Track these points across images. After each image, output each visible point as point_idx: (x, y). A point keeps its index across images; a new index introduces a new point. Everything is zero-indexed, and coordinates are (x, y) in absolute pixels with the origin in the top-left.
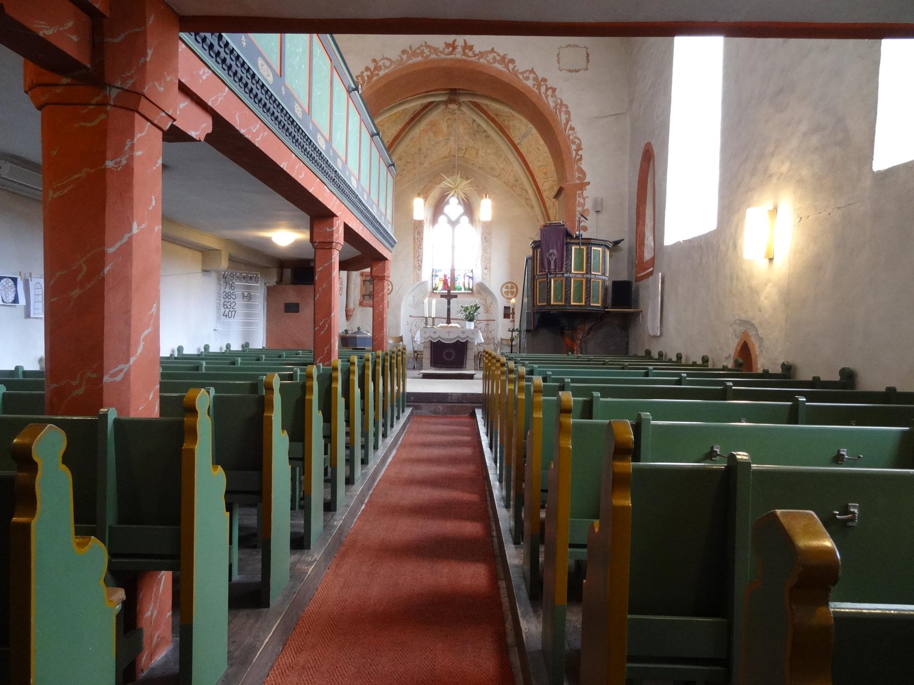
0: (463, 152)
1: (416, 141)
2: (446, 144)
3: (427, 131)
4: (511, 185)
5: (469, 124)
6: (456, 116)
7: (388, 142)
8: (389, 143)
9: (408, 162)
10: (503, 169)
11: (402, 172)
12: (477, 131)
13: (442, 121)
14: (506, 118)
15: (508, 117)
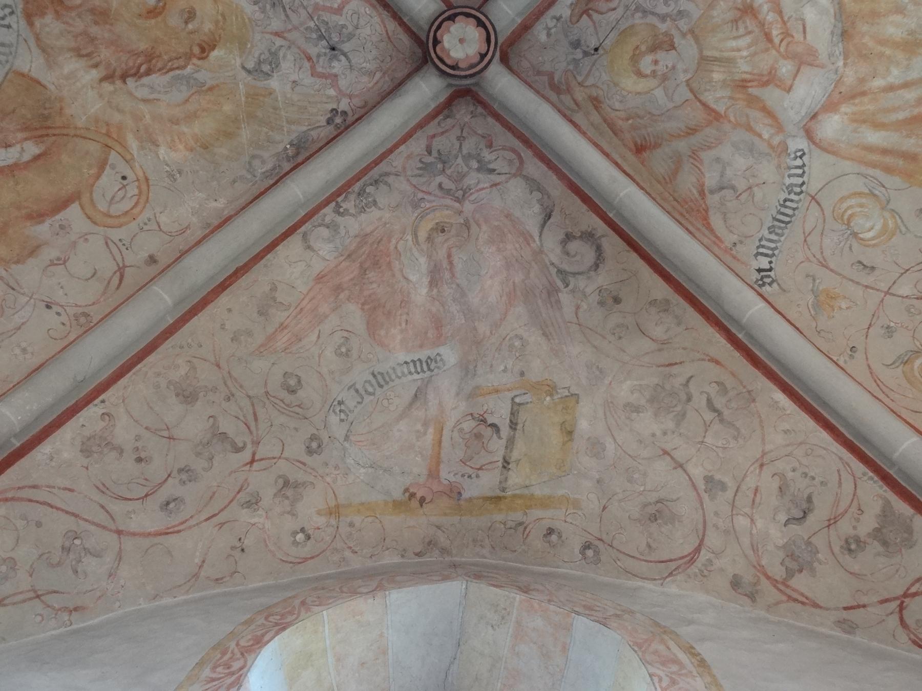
0: (497, 446)
1: (282, 327)
2: (418, 396)
3: (338, 289)
4: (778, 572)
5: (527, 237)
6: (468, 207)
7: (152, 260)
8: (153, 270)
9: (224, 436)
10: (709, 480)
11: (171, 489)
12: (560, 272)
13: (409, 238)
14: (682, 146)
15: (692, 131)
